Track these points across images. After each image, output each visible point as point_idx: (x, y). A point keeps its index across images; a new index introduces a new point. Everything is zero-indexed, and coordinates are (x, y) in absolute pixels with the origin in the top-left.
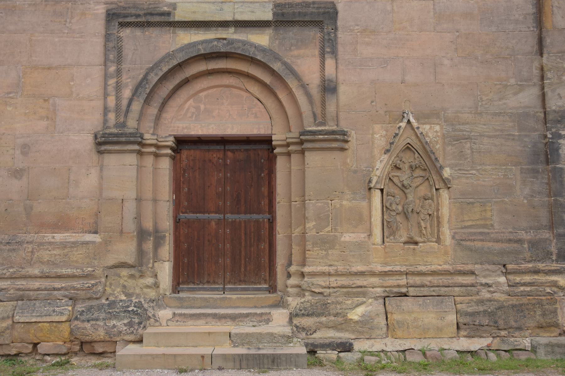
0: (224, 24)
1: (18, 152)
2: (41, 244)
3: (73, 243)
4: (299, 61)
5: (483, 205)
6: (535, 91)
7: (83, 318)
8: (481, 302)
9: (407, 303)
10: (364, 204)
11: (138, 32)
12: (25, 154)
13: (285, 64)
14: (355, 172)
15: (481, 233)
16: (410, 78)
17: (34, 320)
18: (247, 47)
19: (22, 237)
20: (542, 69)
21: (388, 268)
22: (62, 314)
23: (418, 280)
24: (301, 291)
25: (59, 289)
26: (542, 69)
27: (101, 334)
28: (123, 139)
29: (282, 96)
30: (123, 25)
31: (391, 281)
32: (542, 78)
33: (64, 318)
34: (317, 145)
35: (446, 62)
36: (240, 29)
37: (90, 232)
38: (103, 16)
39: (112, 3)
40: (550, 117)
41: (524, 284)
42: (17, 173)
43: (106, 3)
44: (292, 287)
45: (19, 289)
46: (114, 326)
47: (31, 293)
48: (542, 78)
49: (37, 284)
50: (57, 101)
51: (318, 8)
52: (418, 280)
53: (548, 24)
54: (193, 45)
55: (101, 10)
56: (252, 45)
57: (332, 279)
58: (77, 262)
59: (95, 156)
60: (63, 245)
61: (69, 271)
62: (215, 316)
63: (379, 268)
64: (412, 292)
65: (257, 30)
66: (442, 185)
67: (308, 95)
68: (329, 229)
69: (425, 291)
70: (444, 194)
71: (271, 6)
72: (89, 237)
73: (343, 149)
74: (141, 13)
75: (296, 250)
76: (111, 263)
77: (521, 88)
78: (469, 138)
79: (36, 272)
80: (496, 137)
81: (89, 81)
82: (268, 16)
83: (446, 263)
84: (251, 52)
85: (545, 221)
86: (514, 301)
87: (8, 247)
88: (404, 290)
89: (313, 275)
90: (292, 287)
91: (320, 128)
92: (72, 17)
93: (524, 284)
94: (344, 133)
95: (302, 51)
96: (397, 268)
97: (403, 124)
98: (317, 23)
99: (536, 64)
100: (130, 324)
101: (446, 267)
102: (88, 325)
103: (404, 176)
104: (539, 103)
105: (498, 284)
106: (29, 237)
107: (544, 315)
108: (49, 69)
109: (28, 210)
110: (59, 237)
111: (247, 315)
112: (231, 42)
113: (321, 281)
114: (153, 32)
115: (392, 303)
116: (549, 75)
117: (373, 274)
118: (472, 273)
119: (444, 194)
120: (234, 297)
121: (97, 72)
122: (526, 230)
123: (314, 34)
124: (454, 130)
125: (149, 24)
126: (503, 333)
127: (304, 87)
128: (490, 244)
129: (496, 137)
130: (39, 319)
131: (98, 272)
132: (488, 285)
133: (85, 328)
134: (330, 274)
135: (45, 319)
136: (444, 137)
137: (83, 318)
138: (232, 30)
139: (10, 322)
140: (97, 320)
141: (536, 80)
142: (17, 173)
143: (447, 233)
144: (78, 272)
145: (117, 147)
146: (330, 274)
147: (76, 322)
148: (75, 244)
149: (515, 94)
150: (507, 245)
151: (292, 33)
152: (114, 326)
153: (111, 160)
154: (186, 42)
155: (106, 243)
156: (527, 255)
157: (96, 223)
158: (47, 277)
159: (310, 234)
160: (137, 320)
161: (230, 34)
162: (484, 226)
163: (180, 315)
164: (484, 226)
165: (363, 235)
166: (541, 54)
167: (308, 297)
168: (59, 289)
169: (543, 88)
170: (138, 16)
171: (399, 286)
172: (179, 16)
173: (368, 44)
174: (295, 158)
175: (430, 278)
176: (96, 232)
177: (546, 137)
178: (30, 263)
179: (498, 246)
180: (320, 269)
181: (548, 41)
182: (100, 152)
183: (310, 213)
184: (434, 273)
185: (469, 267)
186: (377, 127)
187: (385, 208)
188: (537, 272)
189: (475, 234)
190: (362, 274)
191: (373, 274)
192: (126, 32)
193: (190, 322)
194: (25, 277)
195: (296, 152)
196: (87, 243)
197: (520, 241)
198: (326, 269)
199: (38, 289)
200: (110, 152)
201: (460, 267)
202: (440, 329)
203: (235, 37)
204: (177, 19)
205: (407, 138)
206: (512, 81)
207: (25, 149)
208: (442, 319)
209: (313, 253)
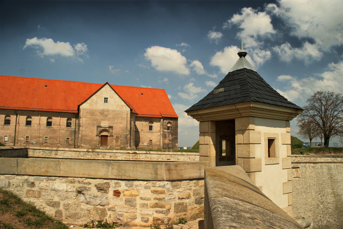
42: (90, 137)
82: (108, 127)
121: (96, 131)
142: (90, 137)
161: (105, 128)
172: (102, 127)
207: (91, 136)
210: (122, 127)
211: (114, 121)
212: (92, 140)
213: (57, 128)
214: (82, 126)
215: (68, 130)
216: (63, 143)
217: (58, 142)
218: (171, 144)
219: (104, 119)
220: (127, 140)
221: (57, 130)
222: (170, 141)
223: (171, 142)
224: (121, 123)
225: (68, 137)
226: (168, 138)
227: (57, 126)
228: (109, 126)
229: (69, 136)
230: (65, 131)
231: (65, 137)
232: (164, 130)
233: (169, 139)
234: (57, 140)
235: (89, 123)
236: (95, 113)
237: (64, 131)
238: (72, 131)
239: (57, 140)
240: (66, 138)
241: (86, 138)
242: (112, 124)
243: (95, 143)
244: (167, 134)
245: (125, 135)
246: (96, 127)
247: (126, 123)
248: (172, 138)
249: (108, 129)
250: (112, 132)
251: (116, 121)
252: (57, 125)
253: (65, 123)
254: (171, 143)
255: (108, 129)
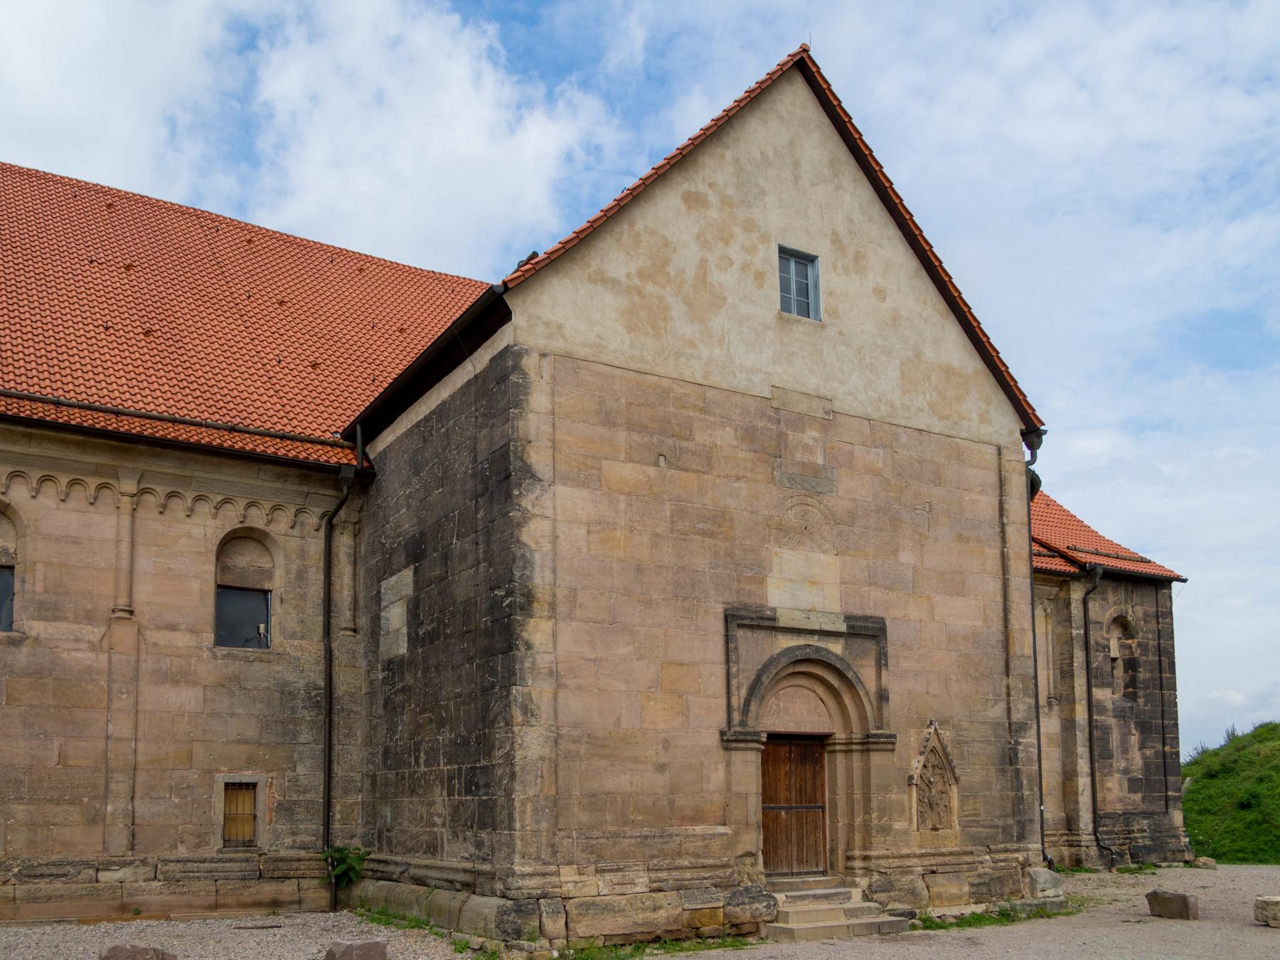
0: (812, 632)
1: (660, 747)
2: (687, 836)
3: (712, 835)
4: (862, 670)
5: (975, 798)
6: (1003, 705)
7: (733, 903)
8: (979, 876)
9: (939, 878)
10: (905, 797)
11: (749, 634)
12: (666, 749)
13: (855, 673)
14: (899, 770)
15: (974, 821)
16: (932, 690)
17: (699, 907)
18: (830, 655)
19: (670, 830)
20: (1008, 687)
21: (923, 851)
22: (718, 900)
23: (940, 860)
24: (868, 871)
25: (707, 879)
26: (1008, 687)
27: (747, 916)
28: (749, 738)
29: (847, 699)
30: (739, 626)
31: (927, 861)
32: (1008, 695)
33: (721, 904)
34: (880, 747)
35: (953, 677)
36: (822, 638)
37: (720, 825)
38: (721, 616)
39: (728, 603)
40: (1013, 727)
41: (1001, 861)
42: (661, 768)
43: (723, 603)
44: (860, 869)
45: (677, 880)
46: (757, 909)
47: (687, 883)
48: (1008, 695)
49: (688, 875)
50: (690, 698)
51: (874, 623)
52: (940, 860)
53: (1012, 652)
54: (790, 650)
55: (720, 609)
56: (828, 652)
57: (890, 861)
58: (715, 852)
59: (722, 752)
60: (704, 837)
61: (711, 861)
62: (815, 896)
63: (918, 851)
64: (940, 869)
65: (833, 639)
66: (953, 781)
67: (870, 701)
68: (886, 819)
69: (947, 869)
70: (955, 789)
71: (843, 618)
72: (722, 829)
73: (893, 750)
74: (754, 616)
75: (858, 837)
76: (740, 852)
77: (996, 702)
78: (966, 742)
79: (686, 863)
80: (982, 742)
81: (713, 679)
82: (843, 628)
83: (956, 846)
84: (833, 661)
85: (1009, 811)
86: (997, 874)
87: (661, 840)
88: (935, 868)
89: (878, 858)
90: (860, 869)
91: (880, 732)
92: (697, 615)
93: (1001, 861)
94: (894, 736)
95: (864, 662)
96: (929, 851)
97: (932, 730)
98: (874, 637)
99: (1004, 683)
100: (768, 907)
101: (957, 849)
102: (738, 909)
103: (929, 773)
104: (1005, 715)
105: (986, 860)
106: (675, 830)
107: (1014, 884)
108: (681, 664)
109: (672, 803)
110: (699, 829)
111: (836, 894)
112: (818, 650)
113: (883, 862)
114: (761, 635)
115: (929, 878)
116: (1013, 693)
117: (915, 856)
118: (972, 853)
119: (955, 789)
120: (811, 879)
122: (999, 817)
123: (870, 645)
124: (959, 735)
125: (759, 627)
126: (994, 899)
127: (867, 694)
128: (980, 830)
129: (982, 742)
130: (703, 906)
131: (732, 862)
132: (981, 862)
133: (736, 912)
134: (888, 857)
135: (707, 906)
136: (952, 741)
137: (733, 903)
138: (816, 637)
139: (680, 910)
140: (744, 904)
141: (1004, 696)
142: (661, 768)
143: (955, 819)
144: (718, 862)
145: (742, 745)
146: (888, 857)
147: (729, 907)
148: (713, 836)
149: (992, 707)
150: (989, 830)
151: (858, 642)
152: (757, 909)
153: (737, 757)
154: (785, 646)
155: (736, 834)
156: (1001, 837)
157: (724, 815)
158: (695, 868)
159: (875, 822)
160: (772, 903)
161: (814, 641)
162: (976, 815)
163: (791, 897)
164: (976, 815)
165: (906, 824)
166: (1008, 676)
167: (876, 877)
168: (707, 879)
169: (1008, 703)
170: (752, 619)
171: (932, 865)
173: (906, 658)
174: (856, 757)
175: (948, 858)
176: (725, 824)
177: (1010, 743)
178: (680, 855)
179: (985, 830)
180: (883, 852)
181: (1012, 665)
182: (726, 749)
183: (874, 804)
184: (951, 854)
185: (969, 849)
186: (913, 731)
187: (920, 801)
188: (1006, 851)
189: (970, 821)
190: (908, 856)
191: (915, 856)
192: (740, 633)
193: (799, 903)
194: (677, 868)
195: (857, 751)
196: (722, 835)
197: (996, 827)
198: (886, 853)
199: (692, 879)
200: (736, 749)
201: (965, 849)
202: (960, 897)
203: (819, 644)
204: (781, 624)
205: (934, 742)
206: (991, 696)
207: (666, 744)
208: (961, 889)
209: (877, 839)
210: (965, 638)
211: (895, 552)
212: (681, 801)
213: (93, 647)
214: (553, 606)
215: (236, 679)
216: (182, 852)
217: (119, 841)
218: (1146, 815)
219: (791, 516)
220: (1019, 787)
221: (89, 670)
222: (1134, 785)
223: (1138, 797)
224: (956, 585)
225: (246, 776)
226: (1123, 764)
227: (93, 632)
228: (848, 618)
229: (251, 762)
230: (199, 692)
231: (209, 773)
232: (1095, 691)
233: (1126, 771)
234: (95, 819)
235: (639, 569)
236: (701, 437)
237: (185, 698)
238: (285, 693)
239: (95, 819)
240: (221, 778)
241: (611, 784)
242: (876, 594)
243: (715, 845)
244: (1112, 721)
245: (996, 725)
246: (720, 626)
247: (999, 585)
248: (1144, 757)
249: (836, 647)
250: (883, 696)
251: (907, 557)
252: (89, 617)
253: (195, 585)
254: (1143, 807)
255: (836, 647)
